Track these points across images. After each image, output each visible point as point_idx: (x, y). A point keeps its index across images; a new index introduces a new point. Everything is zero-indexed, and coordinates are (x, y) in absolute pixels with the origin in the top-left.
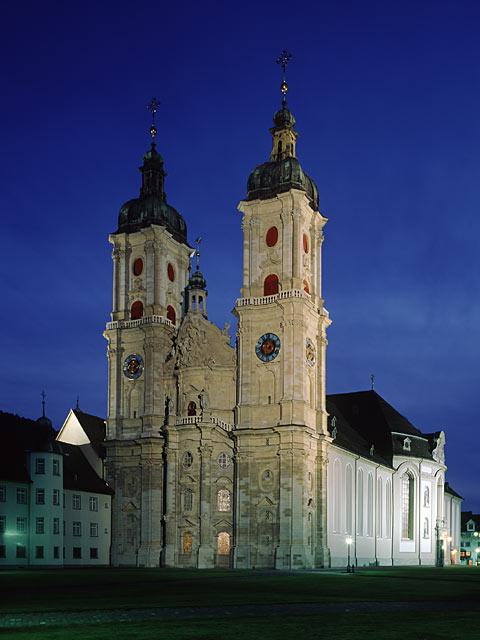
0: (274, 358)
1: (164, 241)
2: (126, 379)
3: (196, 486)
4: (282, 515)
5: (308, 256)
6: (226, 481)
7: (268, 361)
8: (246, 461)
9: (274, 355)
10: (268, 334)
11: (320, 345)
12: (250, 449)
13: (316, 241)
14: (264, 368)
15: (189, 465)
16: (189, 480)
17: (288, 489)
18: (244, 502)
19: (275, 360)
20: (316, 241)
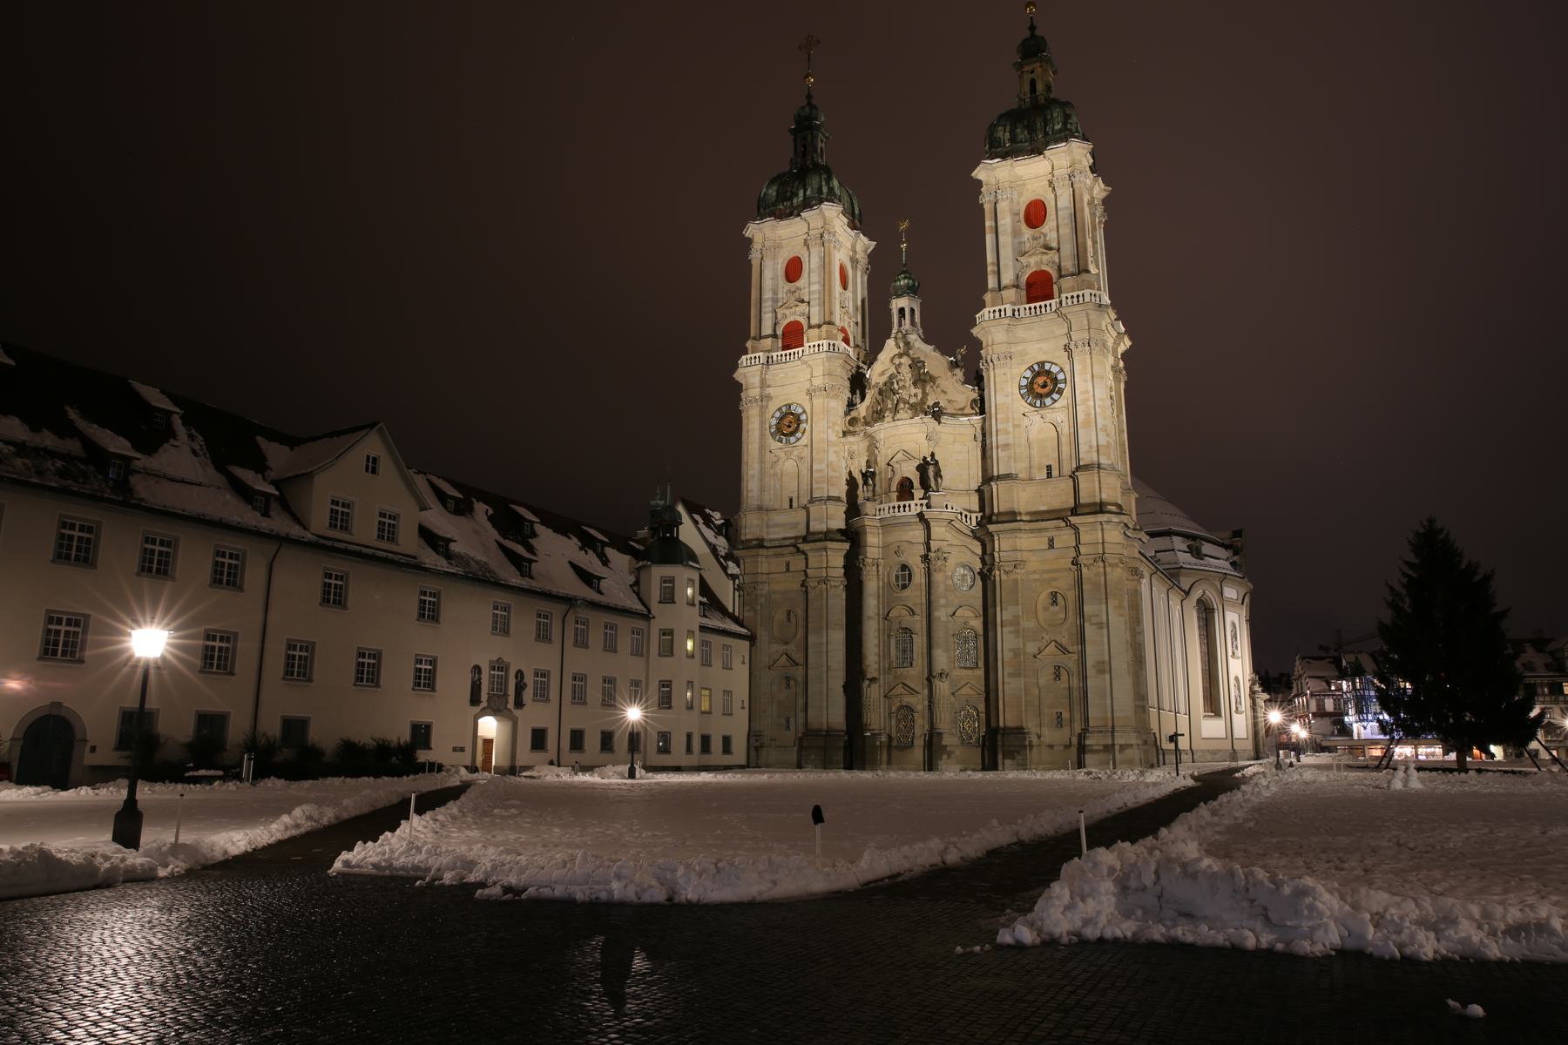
1: (837, 229)
2: (774, 444)
3: (918, 622)
4: (1090, 672)
7: (1043, 405)
9: (1055, 396)
10: (1041, 364)
12: (1019, 556)
13: (1097, 221)
14: (1036, 418)
15: (904, 587)
16: (904, 612)
17: (1100, 625)
18: (1010, 650)
19: (1056, 405)
20: (1097, 221)
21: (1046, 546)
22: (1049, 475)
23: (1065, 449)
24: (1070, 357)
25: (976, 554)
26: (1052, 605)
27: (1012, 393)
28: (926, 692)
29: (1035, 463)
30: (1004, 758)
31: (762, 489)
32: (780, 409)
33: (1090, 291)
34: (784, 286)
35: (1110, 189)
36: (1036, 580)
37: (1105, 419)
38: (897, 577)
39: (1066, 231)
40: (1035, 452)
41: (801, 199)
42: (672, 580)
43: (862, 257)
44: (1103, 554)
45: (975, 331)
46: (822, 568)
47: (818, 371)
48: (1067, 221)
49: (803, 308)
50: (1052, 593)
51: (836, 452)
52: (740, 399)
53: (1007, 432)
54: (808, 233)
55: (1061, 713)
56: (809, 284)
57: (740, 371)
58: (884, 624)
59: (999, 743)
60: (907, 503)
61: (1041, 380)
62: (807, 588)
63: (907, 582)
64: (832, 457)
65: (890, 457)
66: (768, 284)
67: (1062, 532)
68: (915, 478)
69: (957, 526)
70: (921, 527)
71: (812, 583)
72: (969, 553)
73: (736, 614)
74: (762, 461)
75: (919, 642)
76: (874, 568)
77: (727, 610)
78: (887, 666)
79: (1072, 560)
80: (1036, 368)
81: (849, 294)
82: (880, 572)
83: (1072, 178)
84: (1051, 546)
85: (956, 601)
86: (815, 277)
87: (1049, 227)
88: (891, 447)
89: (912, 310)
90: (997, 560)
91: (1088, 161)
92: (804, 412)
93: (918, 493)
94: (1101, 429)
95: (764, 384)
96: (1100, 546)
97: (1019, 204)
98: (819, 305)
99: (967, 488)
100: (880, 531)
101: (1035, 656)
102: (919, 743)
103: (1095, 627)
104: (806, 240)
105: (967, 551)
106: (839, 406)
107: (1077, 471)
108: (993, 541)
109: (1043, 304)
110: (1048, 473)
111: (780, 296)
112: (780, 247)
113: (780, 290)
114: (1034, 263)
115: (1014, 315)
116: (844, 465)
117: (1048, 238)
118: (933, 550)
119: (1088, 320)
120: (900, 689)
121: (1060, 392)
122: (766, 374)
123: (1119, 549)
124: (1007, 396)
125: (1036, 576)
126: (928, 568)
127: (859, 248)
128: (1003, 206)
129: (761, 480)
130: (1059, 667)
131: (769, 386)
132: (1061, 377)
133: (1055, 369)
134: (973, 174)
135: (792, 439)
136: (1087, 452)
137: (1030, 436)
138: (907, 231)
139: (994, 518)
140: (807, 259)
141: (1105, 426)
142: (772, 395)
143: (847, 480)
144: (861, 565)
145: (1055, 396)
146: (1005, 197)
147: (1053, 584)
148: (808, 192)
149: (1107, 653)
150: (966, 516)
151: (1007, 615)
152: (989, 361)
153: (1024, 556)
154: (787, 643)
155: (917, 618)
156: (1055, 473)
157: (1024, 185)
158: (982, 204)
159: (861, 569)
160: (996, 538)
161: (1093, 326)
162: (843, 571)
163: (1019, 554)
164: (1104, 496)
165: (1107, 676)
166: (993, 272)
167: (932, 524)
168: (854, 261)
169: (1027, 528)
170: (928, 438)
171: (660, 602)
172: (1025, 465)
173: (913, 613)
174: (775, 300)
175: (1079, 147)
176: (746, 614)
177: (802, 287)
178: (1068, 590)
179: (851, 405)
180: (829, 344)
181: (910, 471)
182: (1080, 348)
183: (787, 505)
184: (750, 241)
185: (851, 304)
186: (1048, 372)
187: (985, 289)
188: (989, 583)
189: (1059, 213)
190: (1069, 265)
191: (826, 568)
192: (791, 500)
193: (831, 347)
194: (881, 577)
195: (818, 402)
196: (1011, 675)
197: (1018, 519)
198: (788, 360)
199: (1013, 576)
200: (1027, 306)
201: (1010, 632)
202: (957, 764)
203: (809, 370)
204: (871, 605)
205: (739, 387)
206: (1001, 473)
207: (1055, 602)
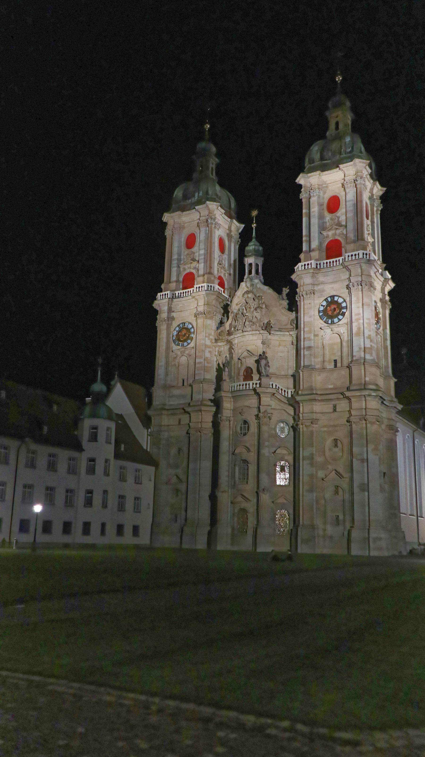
0: (340, 320)
1: (217, 216)
2: (175, 347)
3: (252, 457)
4: (356, 490)
5: (369, 222)
6: (285, 452)
7: (333, 323)
8: (311, 429)
9: (340, 317)
10: (333, 297)
11: (384, 308)
12: (315, 416)
13: (375, 209)
14: (328, 331)
15: (245, 434)
16: (244, 450)
17: (362, 461)
19: (340, 323)
20: (375, 209)
21: (331, 410)
22: (336, 366)
23: (345, 350)
24: (350, 293)
25: (289, 414)
26: (335, 447)
27: (314, 315)
28: (255, 500)
29: (327, 358)
31: (167, 374)
32: (179, 326)
33: (363, 251)
34: (185, 251)
35: (385, 189)
37: (370, 331)
38: (241, 427)
39: (351, 215)
40: (327, 352)
41: (196, 198)
42: (96, 428)
43: (235, 234)
44: (366, 415)
45: (293, 277)
46: (198, 422)
47: (201, 303)
48: (352, 208)
49: (194, 264)
50: (335, 439)
51: (210, 352)
52: (156, 319)
53: (310, 339)
54: (199, 219)
55: (338, 516)
56: (199, 250)
57: (156, 302)
58: (232, 457)
61: (333, 307)
62: (189, 434)
63: (247, 431)
64: (207, 355)
65: (240, 355)
66: (175, 250)
67: (341, 402)
68: (254, 367)
69: (279, 397)
70: (256, 397)
71: (192, 432)
73: (148, 450)
74: (167, 357)
75: (252, 468)
76: (228, 423)
78: (233, 483)
79: (346, 419)
80: (329, 299)
81: (225, 256)
82: (231, 425)
83: (356, 182)
84: (335, 410)
85: (277, 444)
86: (202, 246)
87: (341, 213)
88: (240, 349)
89: (257, 265)
90: (301, 418)
91: (367, 171)
92: (193, 327)
93: (256, 376)
94: (367, 337)
95: (170, 310)
96: (364, 411)
97: (323, 198)
98: (204, 263)
99: (287, 374)
100: (232, 400)
101: (323, 480)
102: (250, 532)
104: (198, 223)
105: (284, 412)
106: (213, 324)
107: (351, 363)
108: (299, 407)
109: (334, 260)
110: (335, 365)
111: (182, 257)
112: (184, 228)
113: (183, 253)
114: (330, 235)
115: (317, 267)
116: (215, 360)
117: (340, 219)
118: (261, 411)
119: (361, 269)
120: (240, 499)
121: (343, 314)
122: (171, 304)
123: (376, 413)
124: (310, 317)
125: (325, 429)
126: (259, 422)
127: (233, 228)
128: (314, 200)
129: (166, 369)
131: (173, 312)
132: (344, 305)
133: (340, 300)
134: (297, 181)
135: (185, 344)
136: (357, 352)
137: (324, 342)
138: (257, 217)
139: (300, 392)
140: (198, 235)
141: (370, 335)
142: (175, 317)
143: (216, 369)
144: (219, 421)
145: (340, 317)
146: (315, 194)
148: (201, 194)
149: (366, 478)
150: (285, 391)
152: (301, 295)
153: (318, 416)
155: (252, 454)
156: (339, 365)
157: (327, 187)
158: (301, 199)
159: (219, 423)
160: (301, 405)
161: (364, 273)
162: (211, 424)
163: (315, 415)
164: (367, 379)
165: (366, 494)
166: (306, 241)
167: (261, 395)
168: (229, 236)
169: (319, 398)
170: (263, 343)
171: (89, 441)
172: (320, 359)
173: (248, 450)
174: (179, 260)
175: (360, 162)
177: (195, 251)
179: (221, 323)
180: (208, 286)
181: (251, 362)
182: (356, 287)
184: (165, 224)
185: (227, 262)
186: (337, 302)
187: (301, 251)
188: (297, 433)
189: (347, 203)
190: (352, 236)
191: (201, 422)
192: (183, 381)
193: (209, 288)
194: (231, 428)
195: (200, 321)
197: (314, 393)
198: (184, 296)
199: (311, 429)
203: (196, 302)
204: (225, 445)
205: (156, 312)
206: (305, 364)
207: (336, 446)
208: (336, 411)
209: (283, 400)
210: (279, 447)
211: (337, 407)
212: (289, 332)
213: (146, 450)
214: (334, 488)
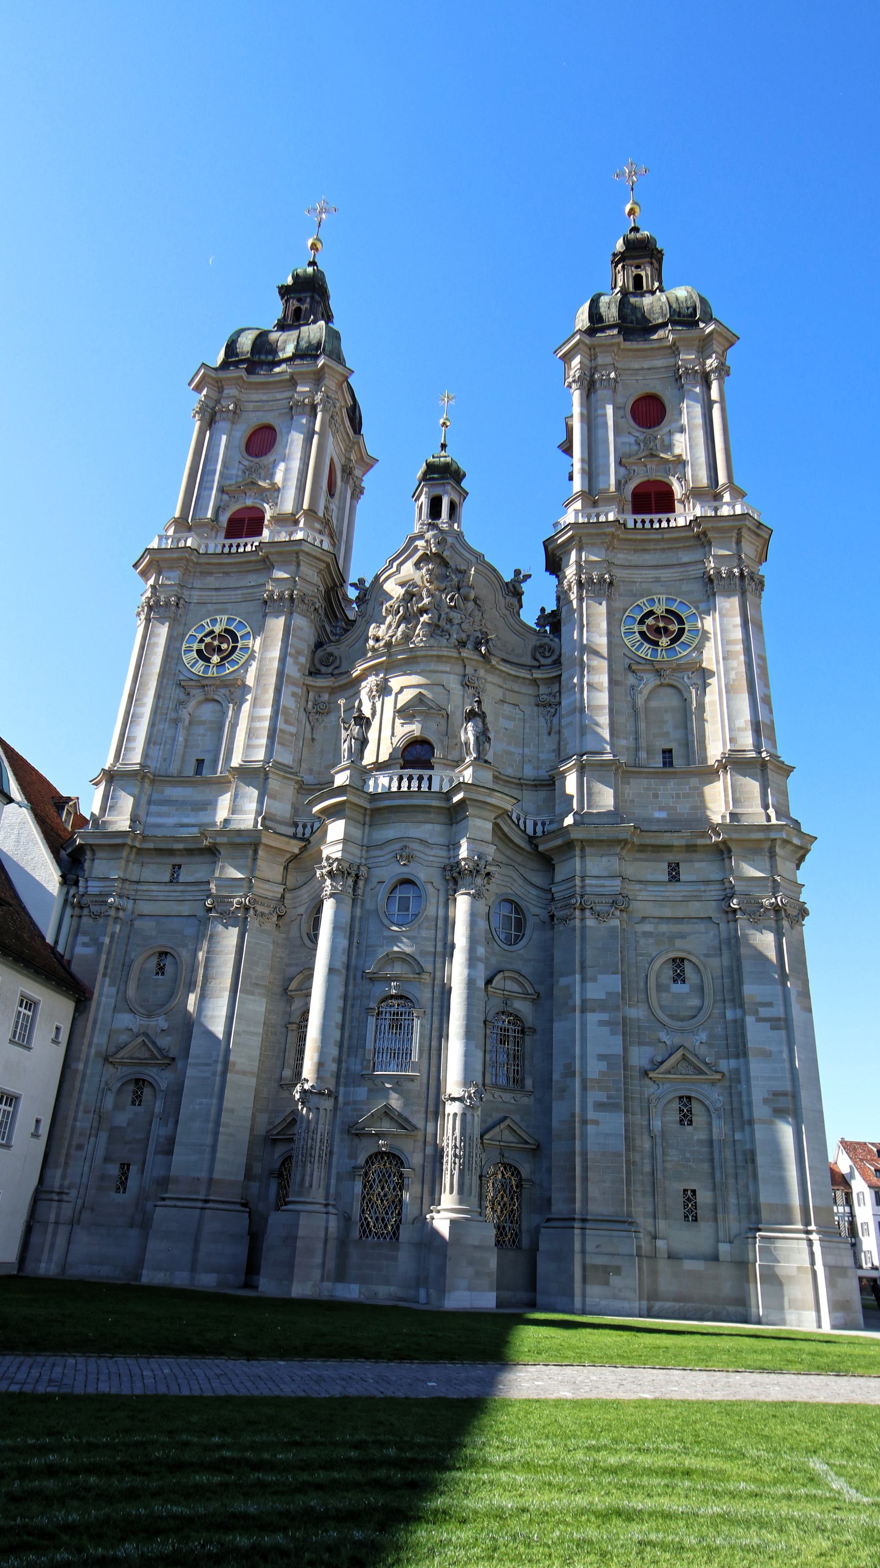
4: (760, 1111)
18: (601, 1057)
21: (666, 878)
26: (675, 981)
30: (584, 1281)
36: (646, 934)
55: (694, 1192)
59: (577, 1246)
60: (426, 773)
72: (520, 881)
73: (60, 949)
77: (43, 938)
99: (519, 775)
103: (768, 1025)
105: (515, 875)
130: (689, 1098)
147: (678, 943)
151: (595, 992)
154: (149, 1015)
176: (79, 950)
178: (707, 955)
183: (190, 770)
196: (600, 1106)
200: (639, 517)
201: (601, 1023)
202: (491, 1290)
207: (680, 978)
208: (679, 880)
209: (517, 840)
210: (500, 971)
211: (682, 869)
212: (533, 671)
213: (53, 949)
214: (676, 1105)
